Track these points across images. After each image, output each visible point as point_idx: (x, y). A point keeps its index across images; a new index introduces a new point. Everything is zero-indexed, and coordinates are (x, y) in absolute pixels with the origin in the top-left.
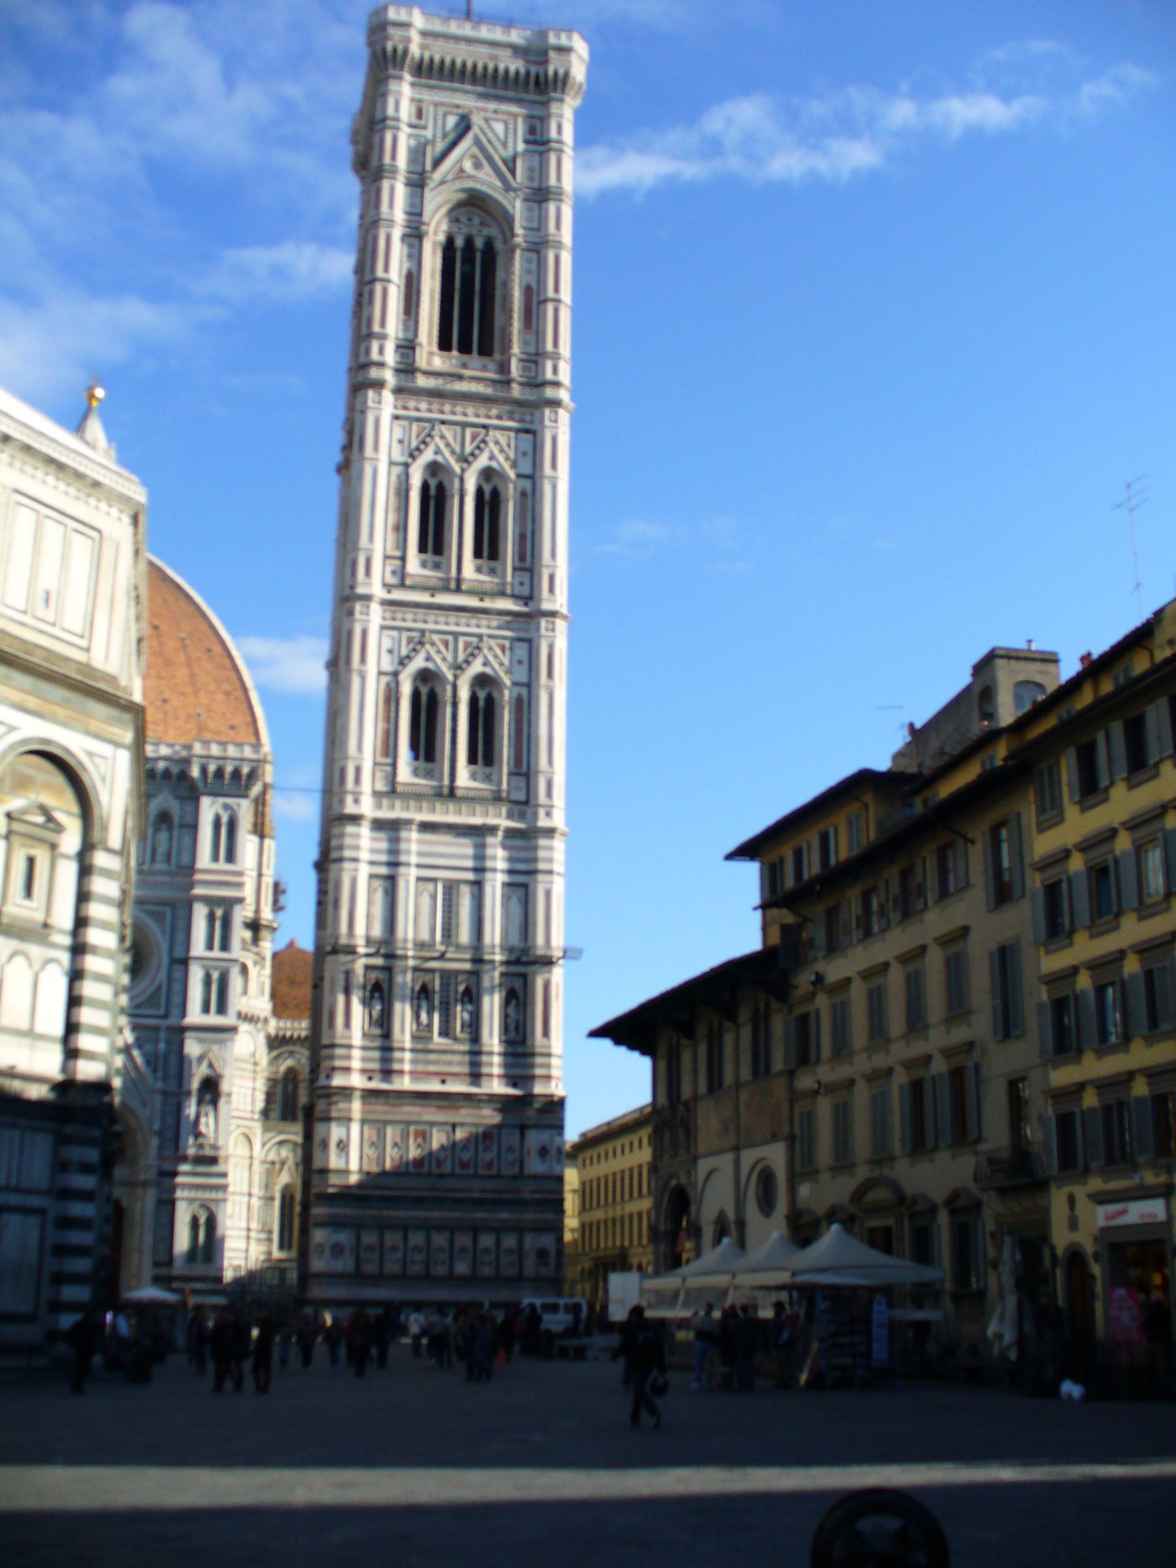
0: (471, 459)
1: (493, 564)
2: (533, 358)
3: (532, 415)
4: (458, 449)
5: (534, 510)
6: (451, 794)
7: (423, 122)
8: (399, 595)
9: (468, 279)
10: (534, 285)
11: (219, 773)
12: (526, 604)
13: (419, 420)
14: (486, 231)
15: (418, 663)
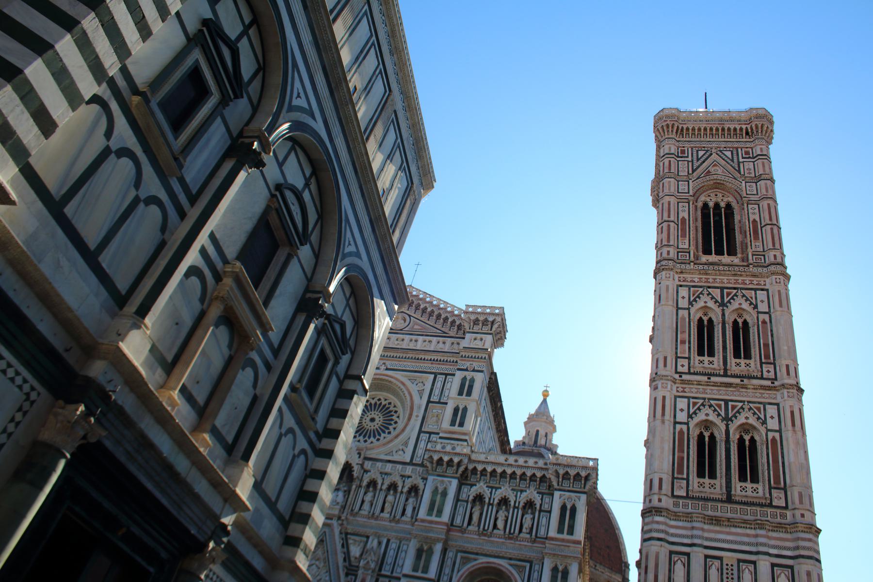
0: (728, 304)
1: (747, 361)
2: (763, 253)
3: (765, 281)
4: (719, 300)
5: (771, 331)
6: (729, 499)
7: (686, 155)
8: (684, 377)
9: (718, 224)
10: (758, 219)
11: (566, 475)
12: (773, 383)
13: (693, 286)
14: (725, 200)
15: (701, 417)
